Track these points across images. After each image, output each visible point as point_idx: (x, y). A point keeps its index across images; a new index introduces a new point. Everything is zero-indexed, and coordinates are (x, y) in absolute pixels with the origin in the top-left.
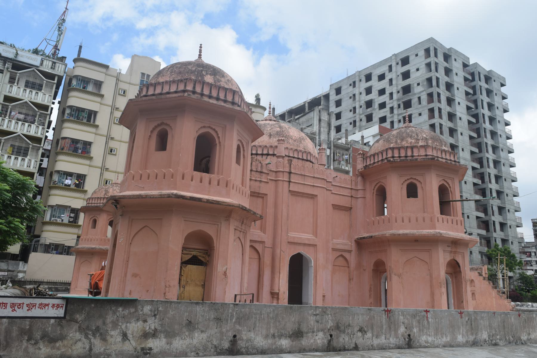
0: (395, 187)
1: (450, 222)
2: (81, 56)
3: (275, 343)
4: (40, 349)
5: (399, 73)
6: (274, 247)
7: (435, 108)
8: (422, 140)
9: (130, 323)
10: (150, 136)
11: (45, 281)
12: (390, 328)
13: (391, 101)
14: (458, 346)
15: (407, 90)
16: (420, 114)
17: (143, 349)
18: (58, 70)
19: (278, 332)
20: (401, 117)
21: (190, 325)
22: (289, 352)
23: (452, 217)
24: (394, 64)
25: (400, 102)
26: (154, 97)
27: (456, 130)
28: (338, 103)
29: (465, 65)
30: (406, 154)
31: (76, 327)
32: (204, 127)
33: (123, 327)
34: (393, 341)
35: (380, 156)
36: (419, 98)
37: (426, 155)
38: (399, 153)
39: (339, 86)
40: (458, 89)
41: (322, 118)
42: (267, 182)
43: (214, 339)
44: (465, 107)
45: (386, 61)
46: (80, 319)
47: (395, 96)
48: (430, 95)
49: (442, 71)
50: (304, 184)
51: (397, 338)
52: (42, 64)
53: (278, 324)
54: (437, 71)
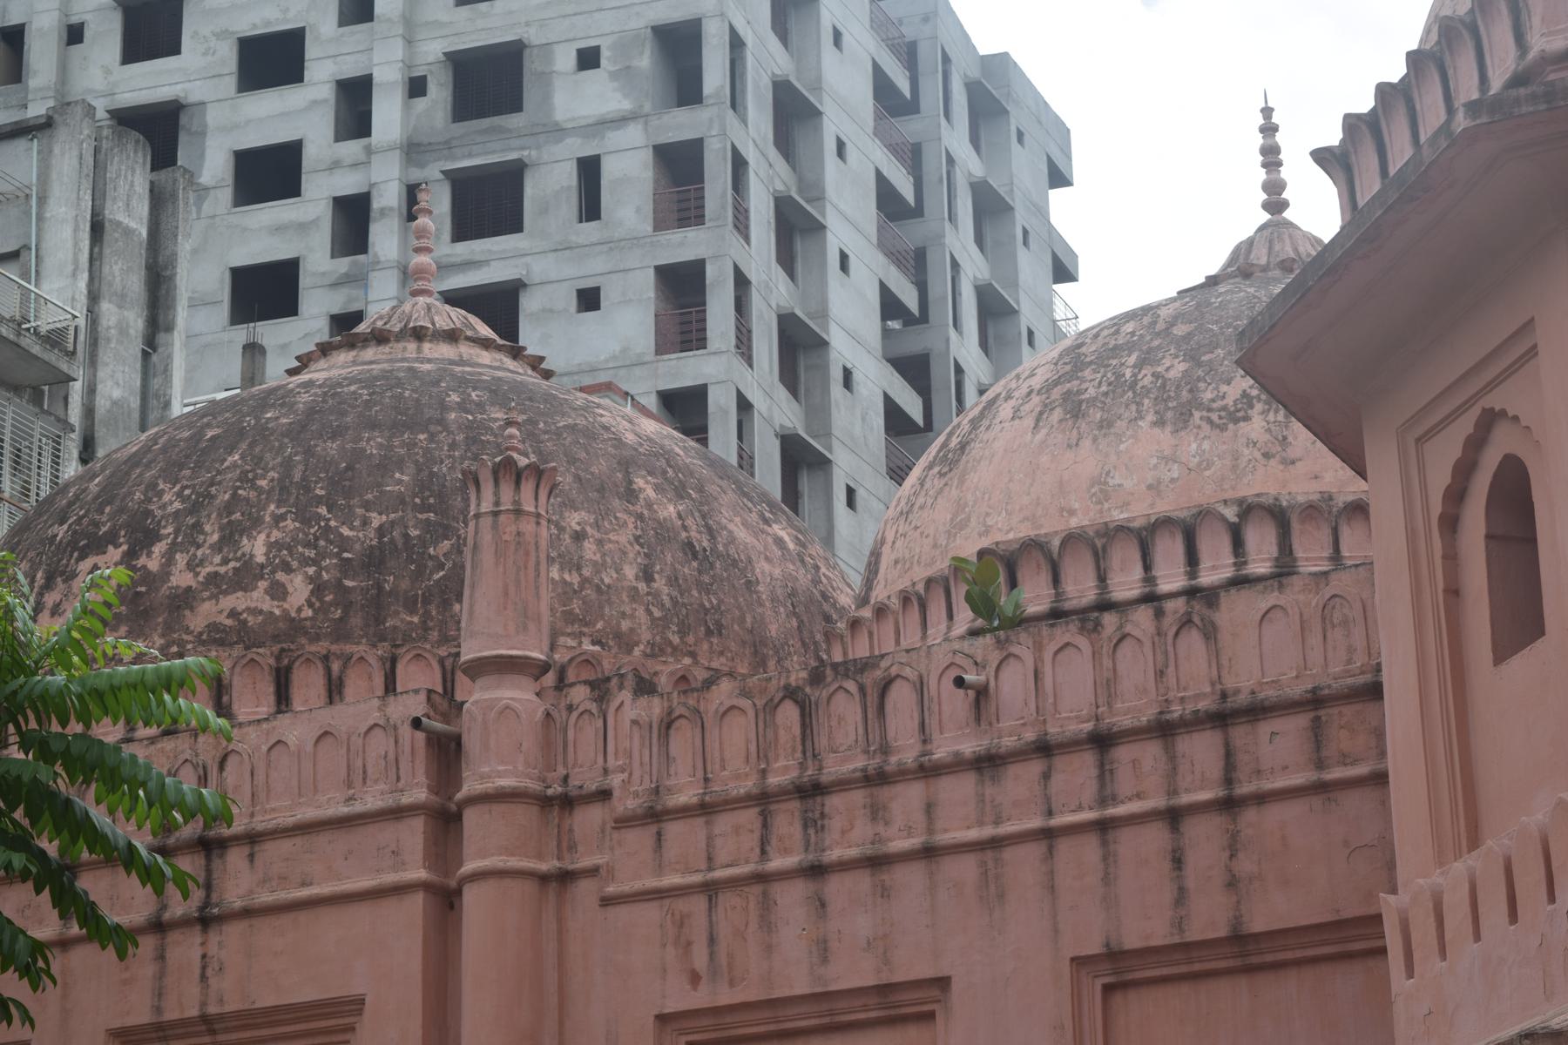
7: (710, 271)
13: (353, 148)
25: (433, 171)
27: (822, 464)
36: (589, 170)
41: (115, 212)
47: (389, 116)
48: (680, 167)
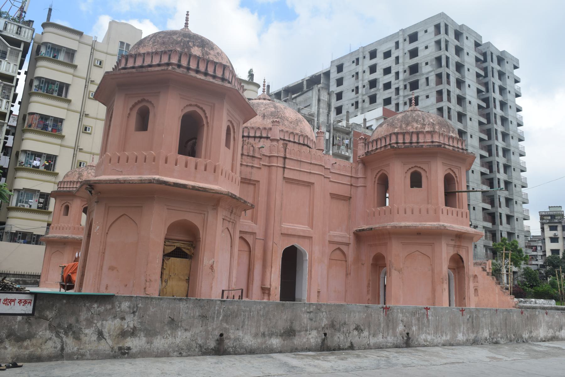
0: (399, 175)
1: (455, 214)
2: (51, 21)
3: (265, 342)
4: (5, 348)
5: (406, 51)
6: (265, 240)
7: (443, 91)
8: (428, 125)
9: (107, 321)
10: (129, 114)
11: (12, 272)
12: (388, 326)
13: (397, 81)
14: (458, 344)
15: (414, 69)
16: (427, 97)
17: (120, 349)
18: (24, 36)
19: (269, 331)
20: (407, 100)
21: (173, 323)
22: (280, 352)
23: (457, 209)
24: (401, 41)
25: (407, 83)
26: (134, 70)
27: (465, 115)
28: (340, 82)
29: (477, 45)
30: (411, 140)
31: (46, 324)
32: (190, 105)
33: (99, 325)
34: (390, 339)
35: (383, 141)
36: (427, 79)
37: (432, 142)
38: (404, 139)
39: (341, 63)
40: (469, 70)
41: (322, 98)
42: (260, 168)
43: (199, 338)
44: (475, 90)
45: (392, 36)
46: (50, 316)
47: (401, 76)
48: (439, 76)
49: (452, 50)
50: (300, 171)
51: (395, 336)
52: (5, 28)
53: (268, 322)
54: (447, 49)
